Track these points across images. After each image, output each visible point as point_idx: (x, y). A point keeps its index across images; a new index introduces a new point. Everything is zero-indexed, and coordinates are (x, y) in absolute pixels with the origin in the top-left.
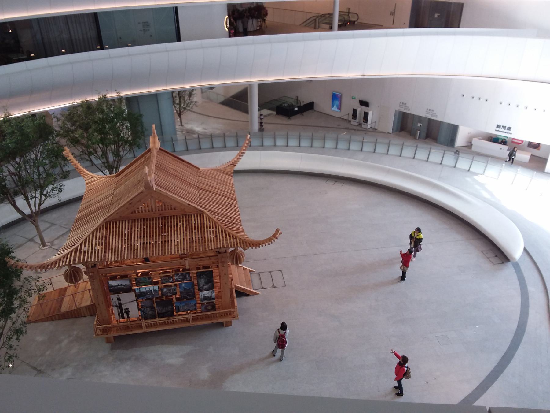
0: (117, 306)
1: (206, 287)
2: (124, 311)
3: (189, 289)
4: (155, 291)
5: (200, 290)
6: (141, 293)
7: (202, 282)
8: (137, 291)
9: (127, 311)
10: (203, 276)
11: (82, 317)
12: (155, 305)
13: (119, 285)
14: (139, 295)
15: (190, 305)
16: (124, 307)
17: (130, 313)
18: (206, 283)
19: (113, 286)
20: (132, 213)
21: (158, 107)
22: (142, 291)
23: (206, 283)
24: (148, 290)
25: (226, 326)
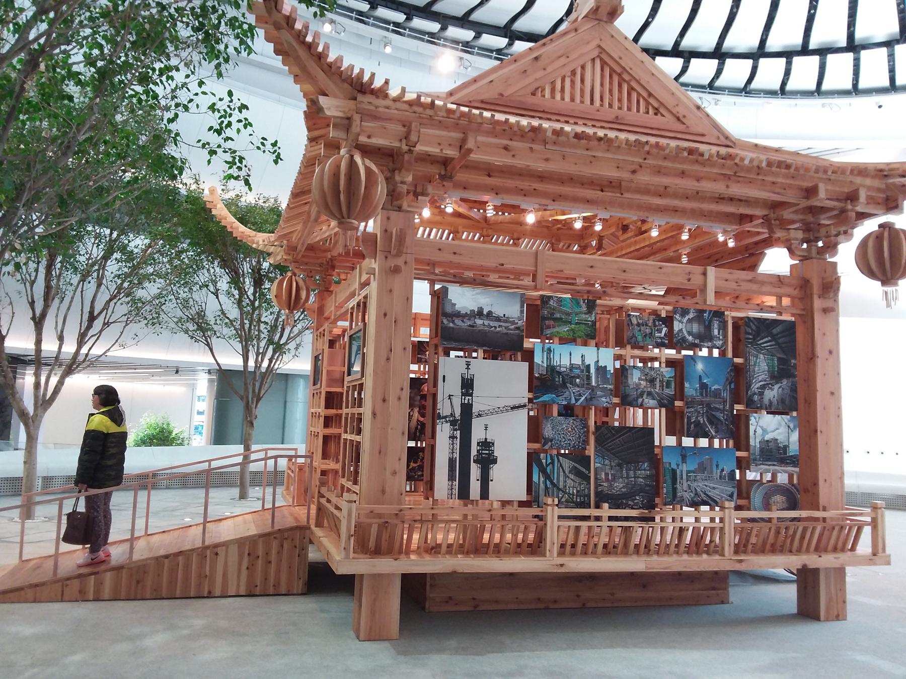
0: (453, 423)
1: (772, 394)
2: (474, 452)
3: (717, 394)
4: (601, 370)
5: (754, 406)
6: (552, 370)
8: (538, 359)
9: (487, 460)
10: (765, 342)
11: (210, 596)
12: (591, 450)
13: (480, 313)
14: (544, 383)
15: (716, 473)
16: (477, 434)
17: (495, 471)
19: (458, 315)
20: (533, 94)
21: (283, 435)
22: (556, 361)
23: (776, 377)
24: (577, 361)
25: (827, 620)
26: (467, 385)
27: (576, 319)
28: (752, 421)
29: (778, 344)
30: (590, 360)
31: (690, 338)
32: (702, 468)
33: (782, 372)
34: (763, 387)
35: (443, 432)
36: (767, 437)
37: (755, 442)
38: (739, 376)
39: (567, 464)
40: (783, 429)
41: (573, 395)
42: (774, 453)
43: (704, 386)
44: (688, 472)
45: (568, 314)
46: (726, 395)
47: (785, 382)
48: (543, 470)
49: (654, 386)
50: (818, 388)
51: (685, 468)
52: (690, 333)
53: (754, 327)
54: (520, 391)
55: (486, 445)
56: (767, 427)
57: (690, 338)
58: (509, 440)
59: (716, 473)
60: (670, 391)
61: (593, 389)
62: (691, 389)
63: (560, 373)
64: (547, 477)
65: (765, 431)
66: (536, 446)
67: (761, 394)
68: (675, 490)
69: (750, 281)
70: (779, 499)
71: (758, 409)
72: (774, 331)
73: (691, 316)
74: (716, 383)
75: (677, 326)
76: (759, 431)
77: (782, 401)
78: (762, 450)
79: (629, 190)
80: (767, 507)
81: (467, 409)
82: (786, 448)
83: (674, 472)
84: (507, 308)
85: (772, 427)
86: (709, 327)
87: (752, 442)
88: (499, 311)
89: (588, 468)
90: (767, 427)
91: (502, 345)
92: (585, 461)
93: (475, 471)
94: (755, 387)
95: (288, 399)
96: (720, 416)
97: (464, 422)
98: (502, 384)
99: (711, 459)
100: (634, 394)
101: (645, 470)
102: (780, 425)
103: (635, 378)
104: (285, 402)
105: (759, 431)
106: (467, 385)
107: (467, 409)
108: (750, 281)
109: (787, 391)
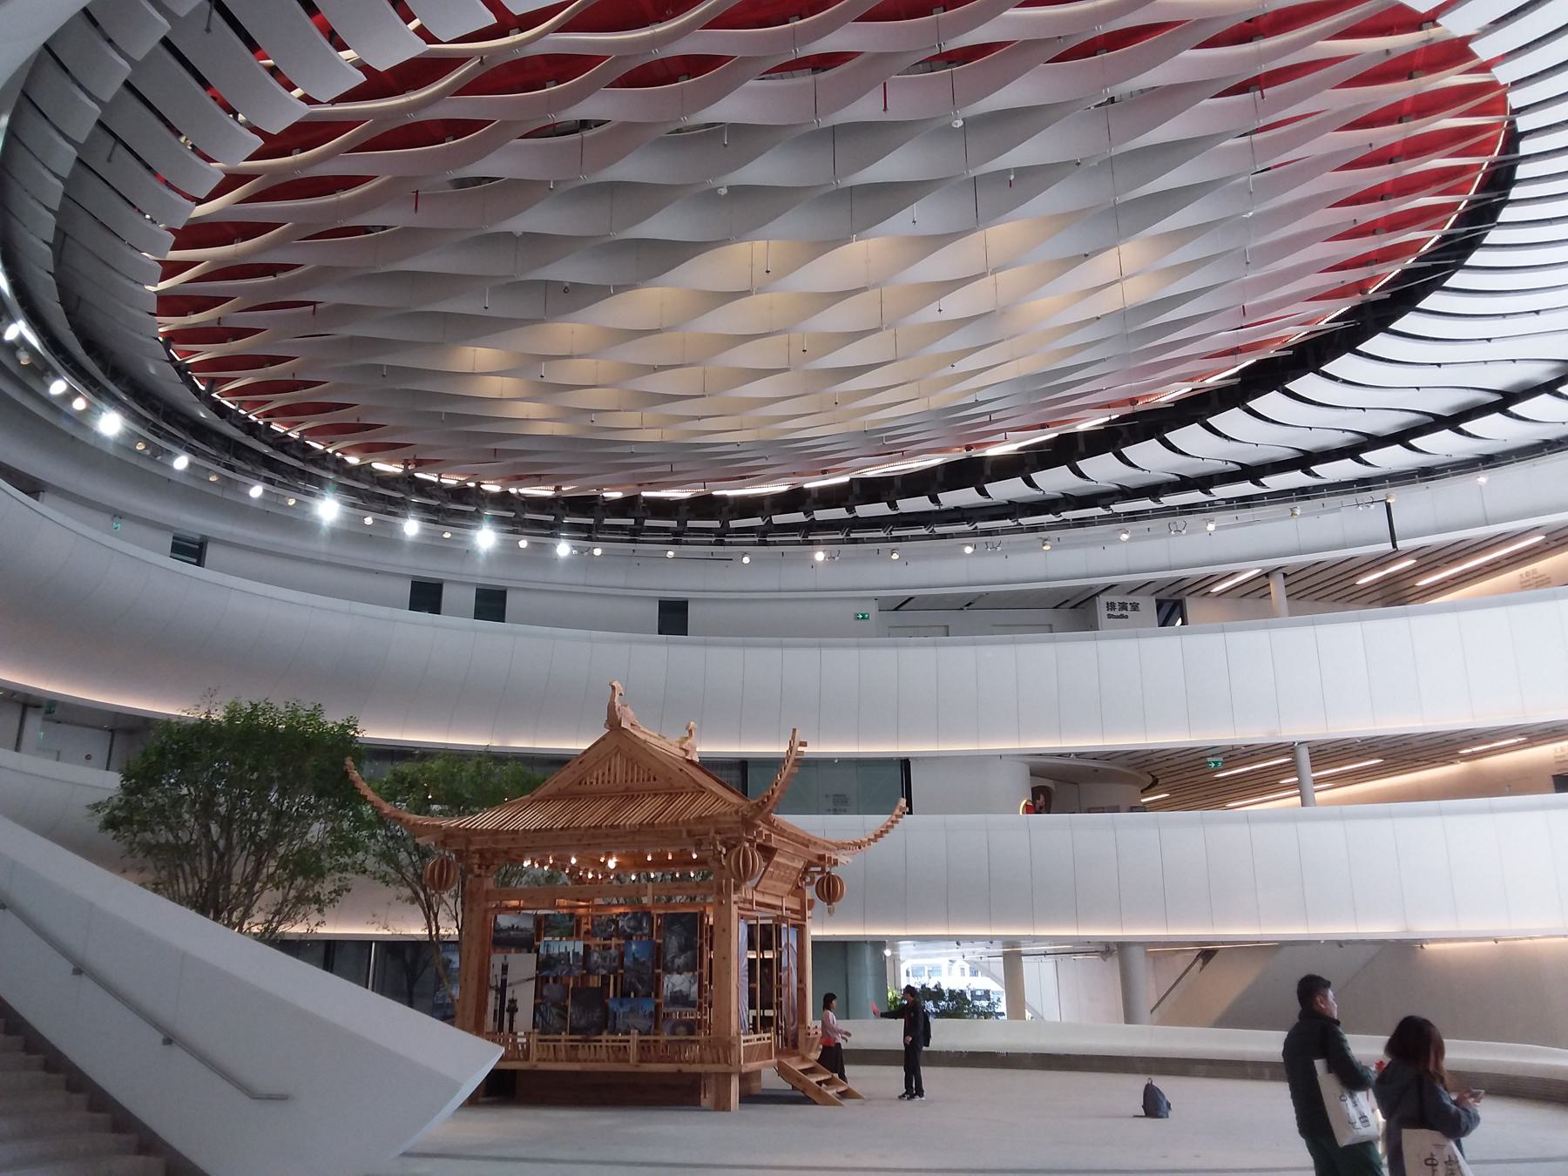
1: (680, 961)
3: (643, 963)
4: (576, 954)
6: (549, 956)
7: (673, 943)
9: (513, 1010)
10: (676, 928)
14: (545, 964)
16: (509, 996)
17: (517, 1016)
18: (682, 950)
23: (682, 950)
26: (505, 969)
30: (570, 950)
32: (632, 1010)
35: (492, 995)
37: (666, 991)
38: (658, 952)
39: (555, 1011)
40: (687, 984)
41: (560, 970)
42: (679, 999)
43: (635, 959)
54: (532, 970)
55: (513, 1001)
56: (676, 982)
58: (525, 997)
62: (627, 961)
70: (681, 1029)
71: (670, 972)
80: (673, 1033)
81: (504, 982)
84: (528, 924)
86: (640, 923)
88: (522, 925)
90: (676, 982)
91: (526, 943)
93: (507, 1016)
94: (669, 957)
97: (502, 991)
98: (523, 965)
101: (598, 1013)
103: (595, 957)
106: (505, 969)
107: (504, 982)
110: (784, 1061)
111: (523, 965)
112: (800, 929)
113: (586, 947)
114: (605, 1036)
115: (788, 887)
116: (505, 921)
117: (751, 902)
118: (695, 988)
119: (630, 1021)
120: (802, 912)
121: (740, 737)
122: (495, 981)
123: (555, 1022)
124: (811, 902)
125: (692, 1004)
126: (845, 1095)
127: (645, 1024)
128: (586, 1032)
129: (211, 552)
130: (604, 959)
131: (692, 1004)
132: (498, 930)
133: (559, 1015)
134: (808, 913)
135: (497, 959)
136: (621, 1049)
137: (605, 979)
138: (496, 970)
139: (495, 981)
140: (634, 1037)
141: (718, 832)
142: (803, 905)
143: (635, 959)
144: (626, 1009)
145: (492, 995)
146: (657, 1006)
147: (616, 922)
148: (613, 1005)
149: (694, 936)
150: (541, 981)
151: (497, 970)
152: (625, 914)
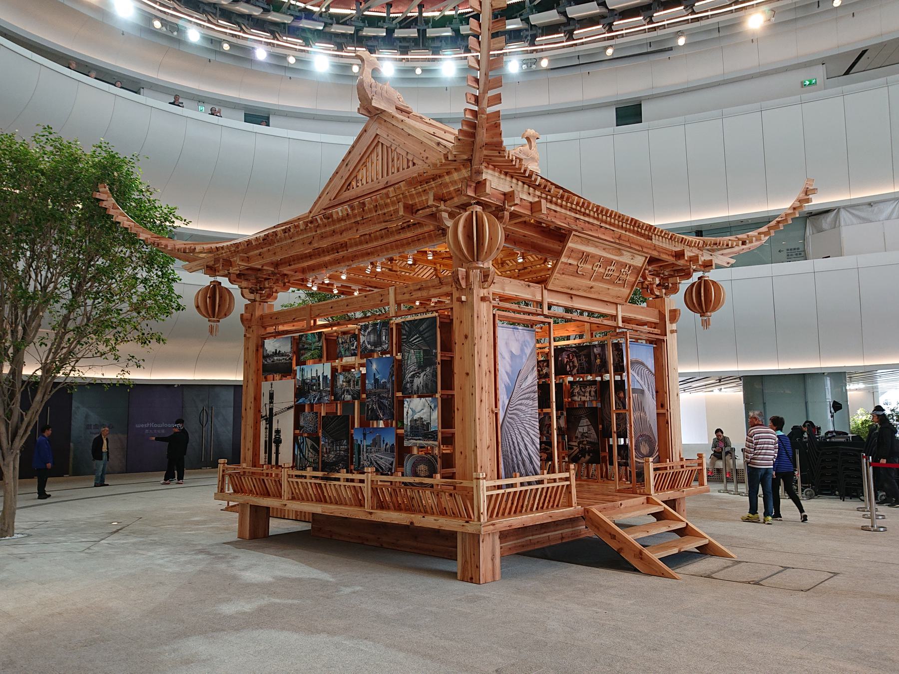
0: (266, 420)
1: (418, 381)
3: (384, 386)
4: (325, 377)
6: (303, 380)
7: (412, 358)
9: (278, 442)
10: (415, 339)
12: (320, 434)
13: (276, 353)
14: (302, 390)
15: (383, 446)
16: (275, 427)
17: (282, 447)
18: (421, 367)
23: (421, 367)
27: (313, 347)
28: (406, 404)
29: (423, 339)
30: (320, 374)
31: (369, 346)
32: (375, 443)
33: (426, 362)
34: (413, 376)
36: (416, 417)
37: (407, 421)
39: (309, 442)
40: (427, 410)
42: (421, 429)
43: (376, 380)
44: (367, 446)
45: (310, 344)
46: (389, 386)
47: (428, 369)
48: (299, 447)
49: (350, 385)
50: (456, 371)
51: (365, 443)
52: (369, 343)
53: (407, 329)
55: (278, 432)
56: (418, 408)
57: (369, 346)
59: (383, 446)
60: (358, 388)
61: (321, 391)
63: (307, 384)
64: (301, 451)
65: (413, 411)
66: (297, 432)
67: (412, 382)
68: (359, 459)
69: (419, 289)
70: (422, 468)
72: (421, 329)
73: (370, 329)
74: (383, 377)
75: (362, 339)
76: (410, 412)
77: (426, 385)
78: (412, 427)
79: (351, 246)
80: (415, 474)
81: (271, 410)
82: (429, 424)
83: (359, 446)
85: (419, 408)
86: (380, 336)
87: (405, 422)
89: (318, 444)
90: (418, 408)
92: (317, 440)
94: (408, 377)
95: (809, 400)
96: (386, 402)
97: (270, 421)
99: (380, 436)
100: (340, 392)
102: (424, 406)
103: (341, 379)
104: (806, 403)
105: (410, 412)
107: (271, 410)
108: (419, 289)
109: (430, 377)
110: (594, 509)
111: (283, 391)
112: (658, 345)
113: (334, 370)
114: (343, 474)
115: (626, 291)
116: (271, 345)
117: (540, 304)
118: (436, 416)
119: (373, 456)
120: (661, 325)
121: (690, 206)
122: (265, 412)
123: (310, 455)
124: (674, 315)
125: (433, 436)
126: (706, 551)
127: (385, 460)
128: (328, 467)
129: (272, 120)
130: (349, 382)
131: (433, 436)
132: (266, 357)
133: (313, 447)
134: (670, 327)
135: (266, 387)
136: (357, 492)
137: (348, 406)
138: (265, 399)
139: (265, 412)
140: (370, 475)
141: (440, 198)
142: (662, 316)
143: (376, 380)
144: (368, 442)
145: (263, 424)
146: (400, 439)
147: (356, 337)
148: (358, 437)
149: (435, 346)
150: (299, 410)
151: (265, 399)
152: (366, 327)
